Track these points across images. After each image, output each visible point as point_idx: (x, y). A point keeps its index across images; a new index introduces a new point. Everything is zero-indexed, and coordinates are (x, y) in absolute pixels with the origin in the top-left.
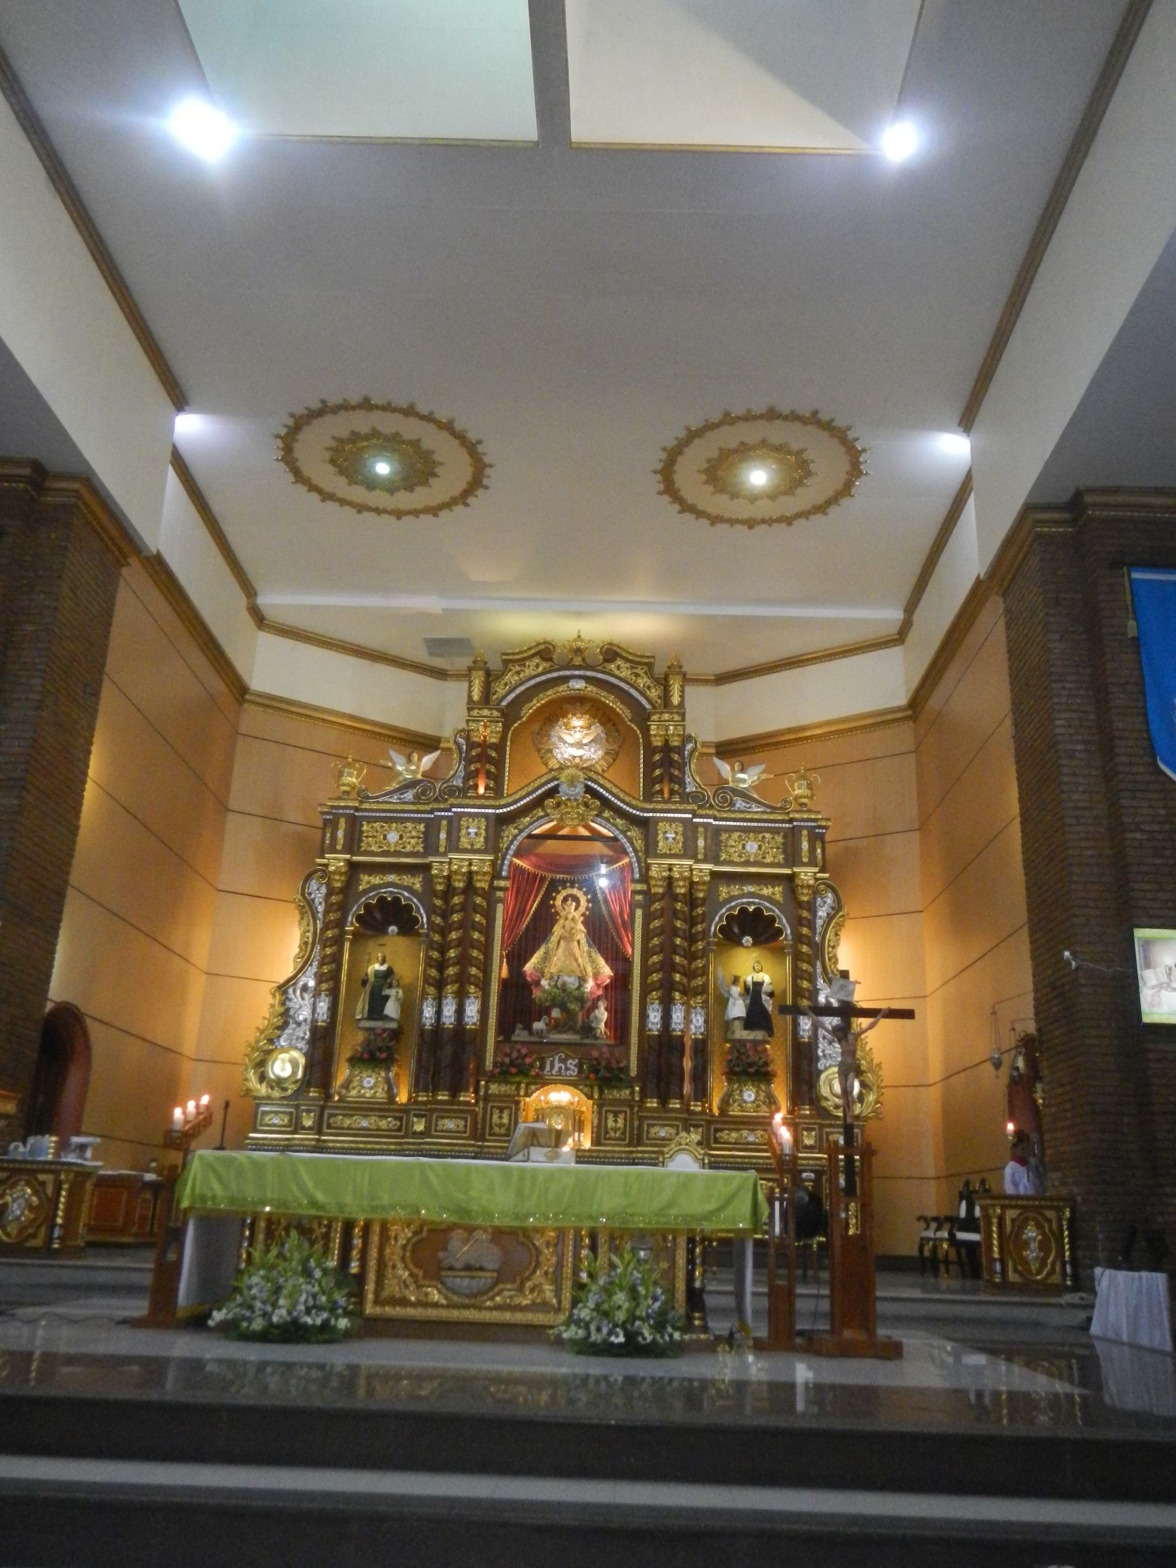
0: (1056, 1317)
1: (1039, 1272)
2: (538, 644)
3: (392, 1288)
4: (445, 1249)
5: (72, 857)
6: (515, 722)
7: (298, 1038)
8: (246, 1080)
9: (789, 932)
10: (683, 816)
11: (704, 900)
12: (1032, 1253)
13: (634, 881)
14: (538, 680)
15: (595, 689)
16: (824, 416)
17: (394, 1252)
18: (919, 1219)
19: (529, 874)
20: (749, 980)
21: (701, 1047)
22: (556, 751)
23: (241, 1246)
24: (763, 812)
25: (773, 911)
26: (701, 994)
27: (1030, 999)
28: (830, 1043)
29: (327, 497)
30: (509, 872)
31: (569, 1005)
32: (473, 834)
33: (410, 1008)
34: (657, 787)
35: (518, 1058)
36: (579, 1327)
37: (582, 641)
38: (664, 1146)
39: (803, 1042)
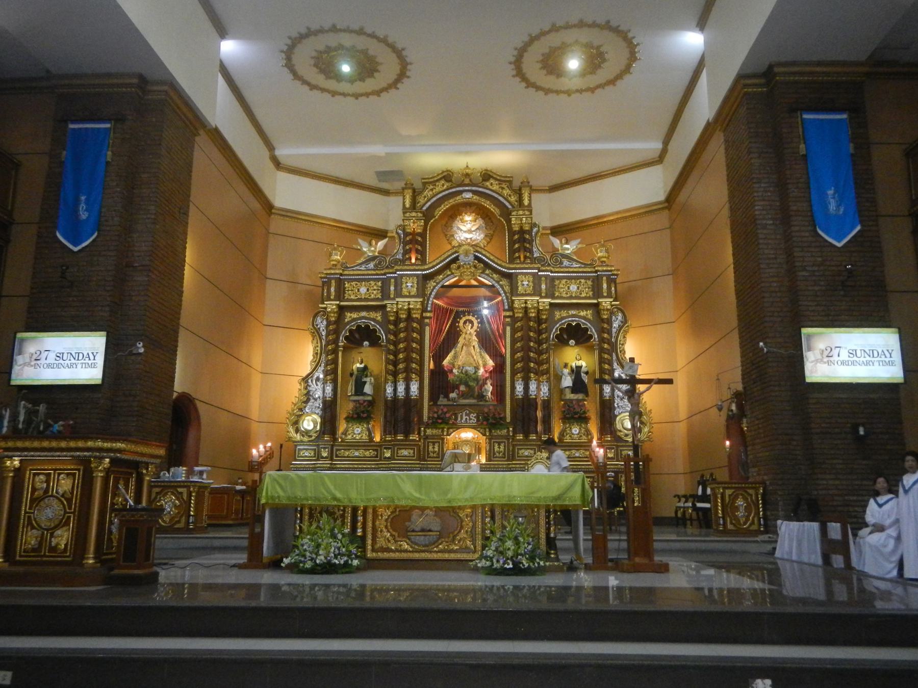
0: (753, 548)
1: (745, 523)
2: (443, 172)
3: (381, 542)
4: (409, 520)
5: (180, 309)
6: (431, 219)
7: (316, 407)
8: (288, 432)
9: (596, 336)
10: (532, 271)
11: (546, 319)
12: (740, 514)
13: (504, 310)
14: (444, 193)
15: (478, 198)
16: (614, 24)
17: (381, 524)
18: (675, 496)
19: (443, 308)
20: (574, 365)
21: (547, 404)
22: (456, 236)
23: (295, 523)
25: (587, 325)
26: (546, 374)
27: (739, 372)
28: (622, 399)
29: (313, 87)
30: (432, 308)
31: (469, 383)
32: (409, 287)
33: (378, 388)
34: (517, 255)
35: (441, 414)
36: (487, 560)
37: (469, 169)
38: (528, 460)
39: (607, 400)
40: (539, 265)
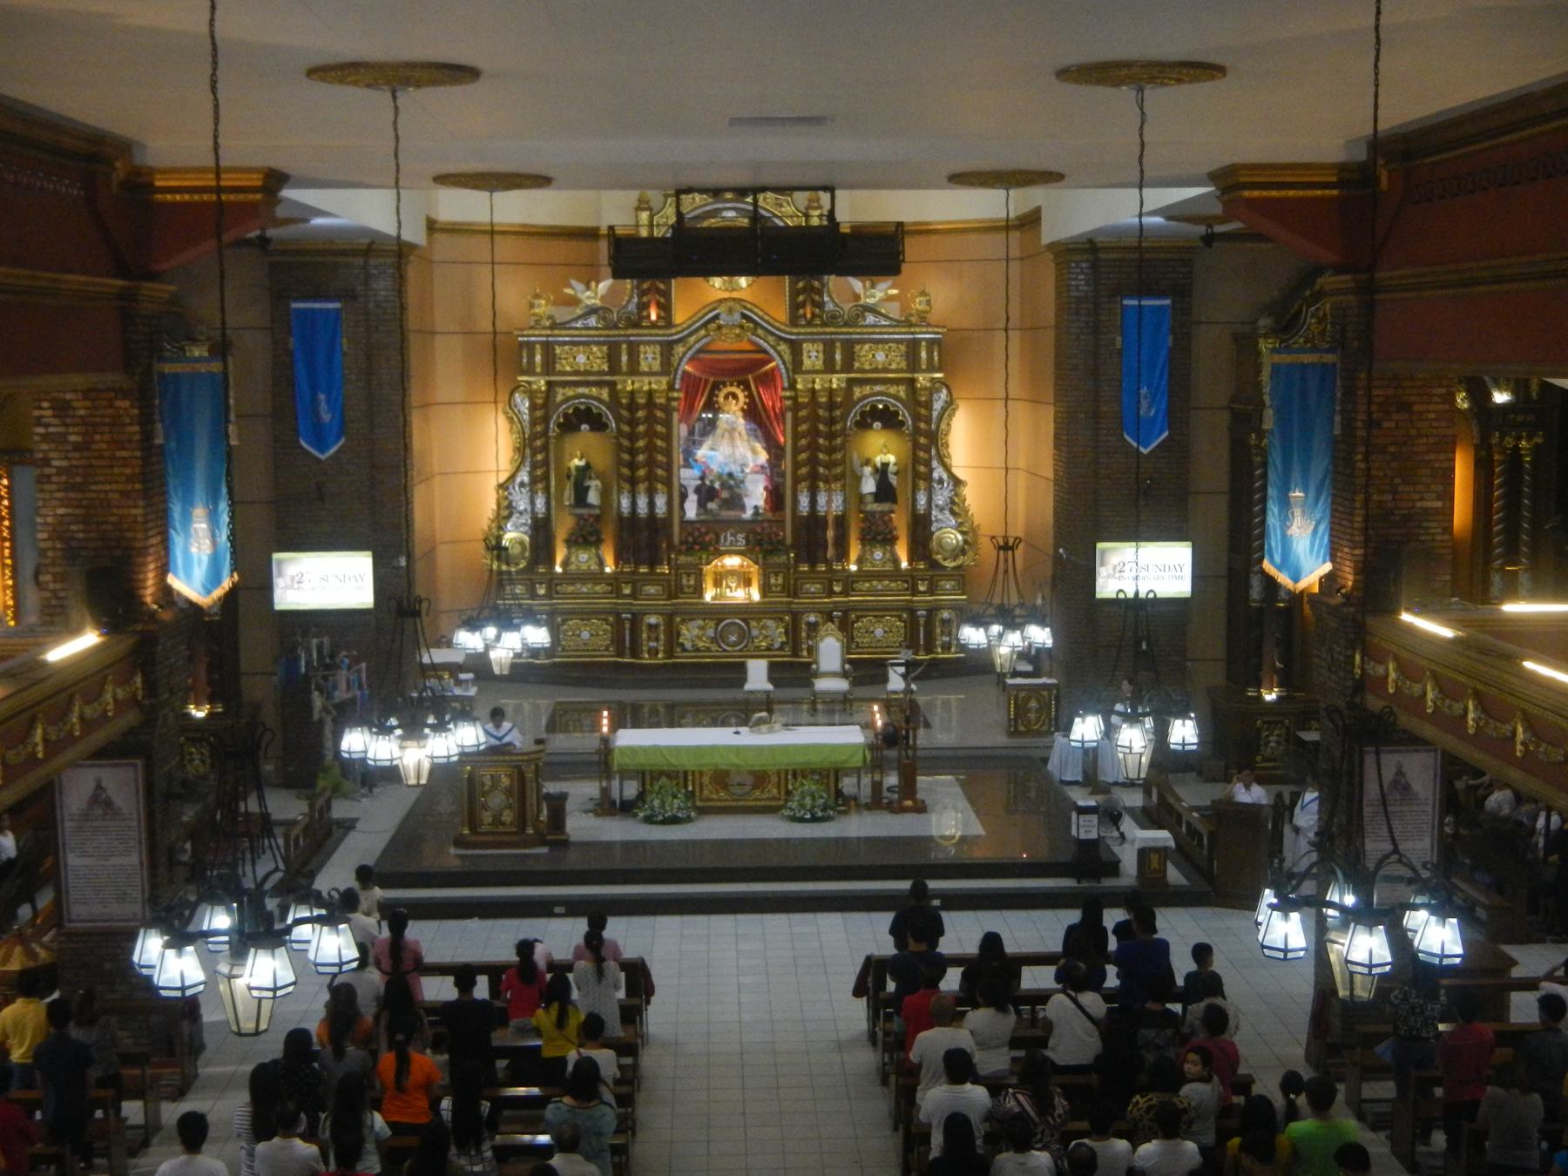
3: (706, 792)
12: (1032, 716)
13: (784, 389)
17: (706, 780)
20: (878, 460)
21: (841, 522)
24: (889, 326)
34: (801, 311)
40: (832, 329)
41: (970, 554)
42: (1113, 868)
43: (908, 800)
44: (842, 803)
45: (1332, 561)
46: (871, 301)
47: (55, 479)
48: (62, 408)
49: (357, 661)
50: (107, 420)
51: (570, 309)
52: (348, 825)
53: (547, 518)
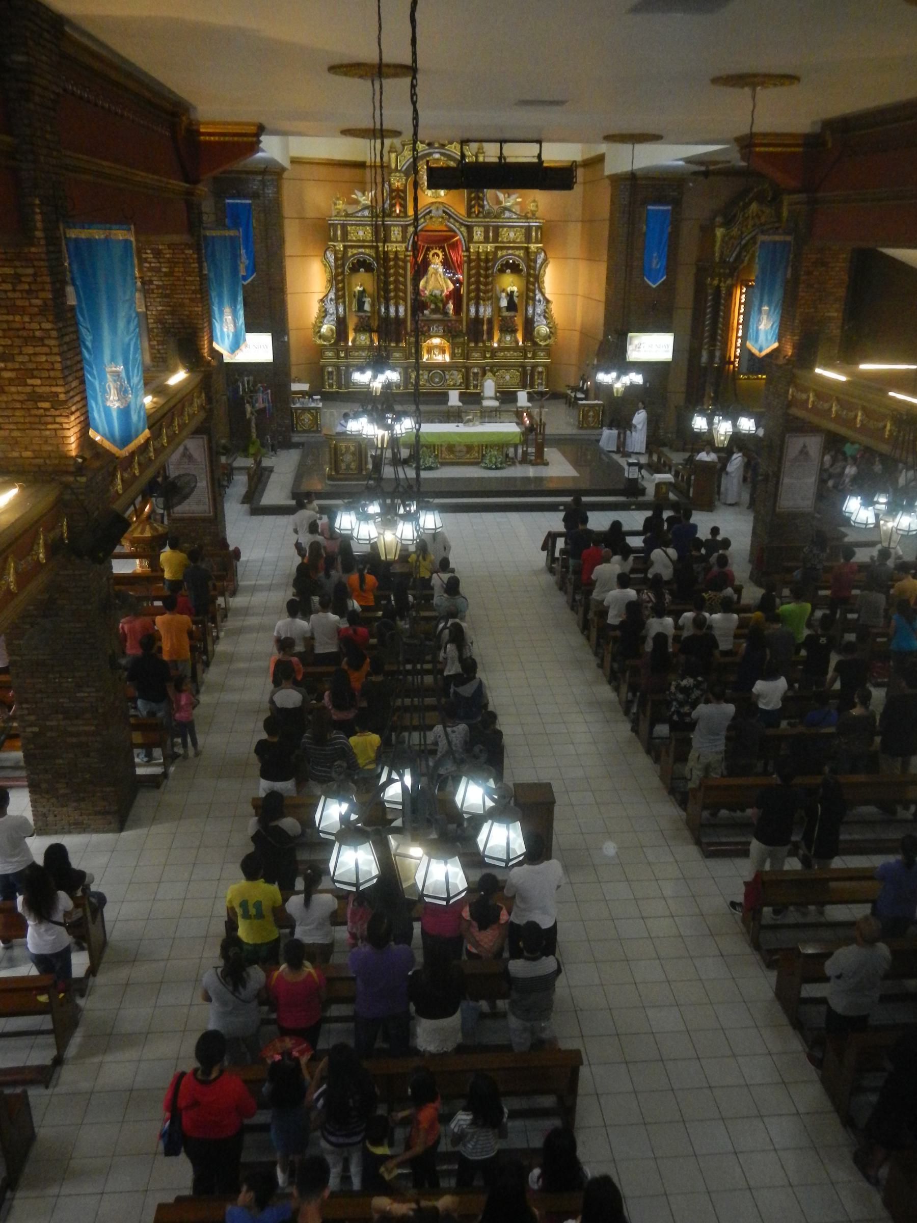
3: (443, 455)
12: (590, 419)
13: (463, 251)
17: (444, 449)
20: (509, 289)
21: (490, 321)
24: (518, 218)
28: (540, 316)
34: (473, 210)
40: (488, 220)
41: (553, 338)
42: (643, 492)
43: (540, 460)
44: (509, 461)
45: (779, 341)
46: (508, 204)
47: (155, 291)
48: (157, 254)
49: (265, 389)
50: (181, 260)
51: (354, 206)
52: (270, 470)
53: (345, 317)
